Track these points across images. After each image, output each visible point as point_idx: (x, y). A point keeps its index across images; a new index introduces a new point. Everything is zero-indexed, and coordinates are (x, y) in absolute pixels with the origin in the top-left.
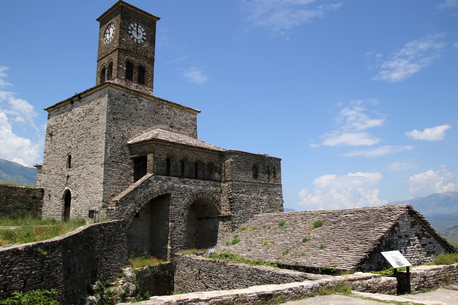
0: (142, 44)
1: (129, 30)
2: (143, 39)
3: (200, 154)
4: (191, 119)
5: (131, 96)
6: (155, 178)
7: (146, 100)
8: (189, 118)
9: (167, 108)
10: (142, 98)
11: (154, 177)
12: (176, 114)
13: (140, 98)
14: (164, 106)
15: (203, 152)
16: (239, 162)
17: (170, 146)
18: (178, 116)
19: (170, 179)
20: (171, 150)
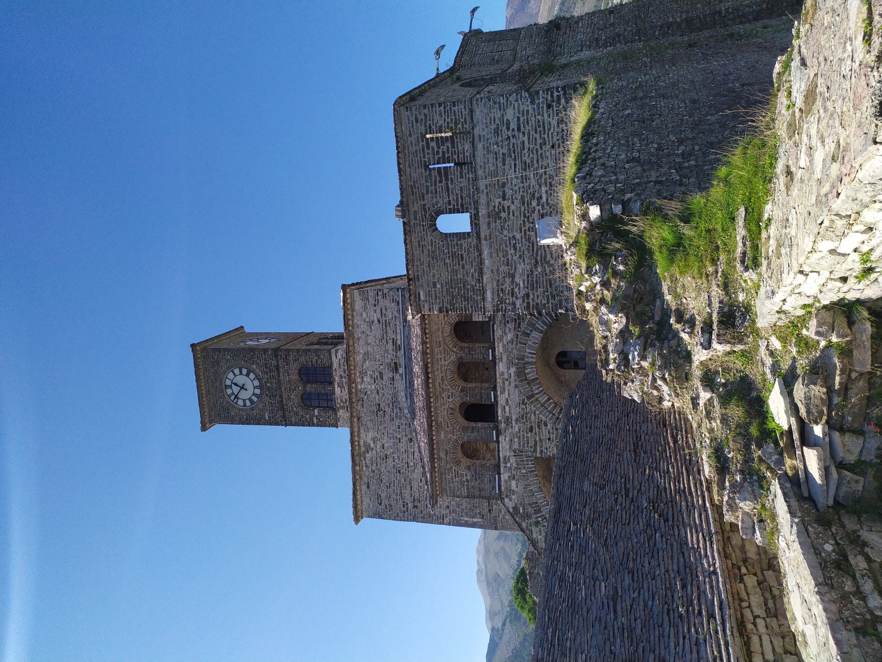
0: (257, 377)
1: (245, 405)
2: (250, 400)
3: (439, 375)
4: (365, 308)
5: (364, 468)
6: (507, 496)
7: (363, 435)
8: (364, 315)
9: (362, 378)
10: (362, 443)
11: (507, 500)
12: (367, 354)
13: (363, 449)
14: (359, 387)
15: (432, 364)
16: (435, 286)
17: (440, 458)
18: (370, 349)
19: (505, 458)
20: (446, 455)
